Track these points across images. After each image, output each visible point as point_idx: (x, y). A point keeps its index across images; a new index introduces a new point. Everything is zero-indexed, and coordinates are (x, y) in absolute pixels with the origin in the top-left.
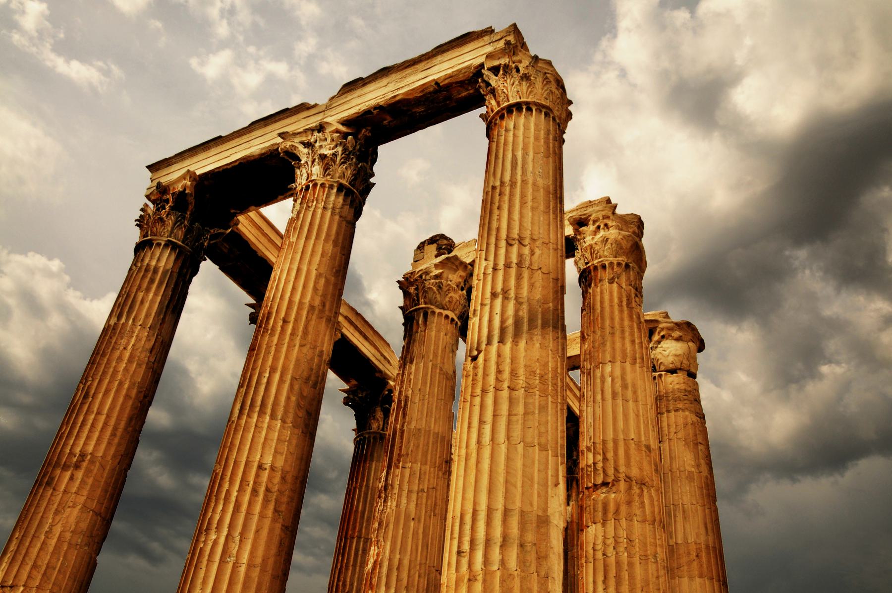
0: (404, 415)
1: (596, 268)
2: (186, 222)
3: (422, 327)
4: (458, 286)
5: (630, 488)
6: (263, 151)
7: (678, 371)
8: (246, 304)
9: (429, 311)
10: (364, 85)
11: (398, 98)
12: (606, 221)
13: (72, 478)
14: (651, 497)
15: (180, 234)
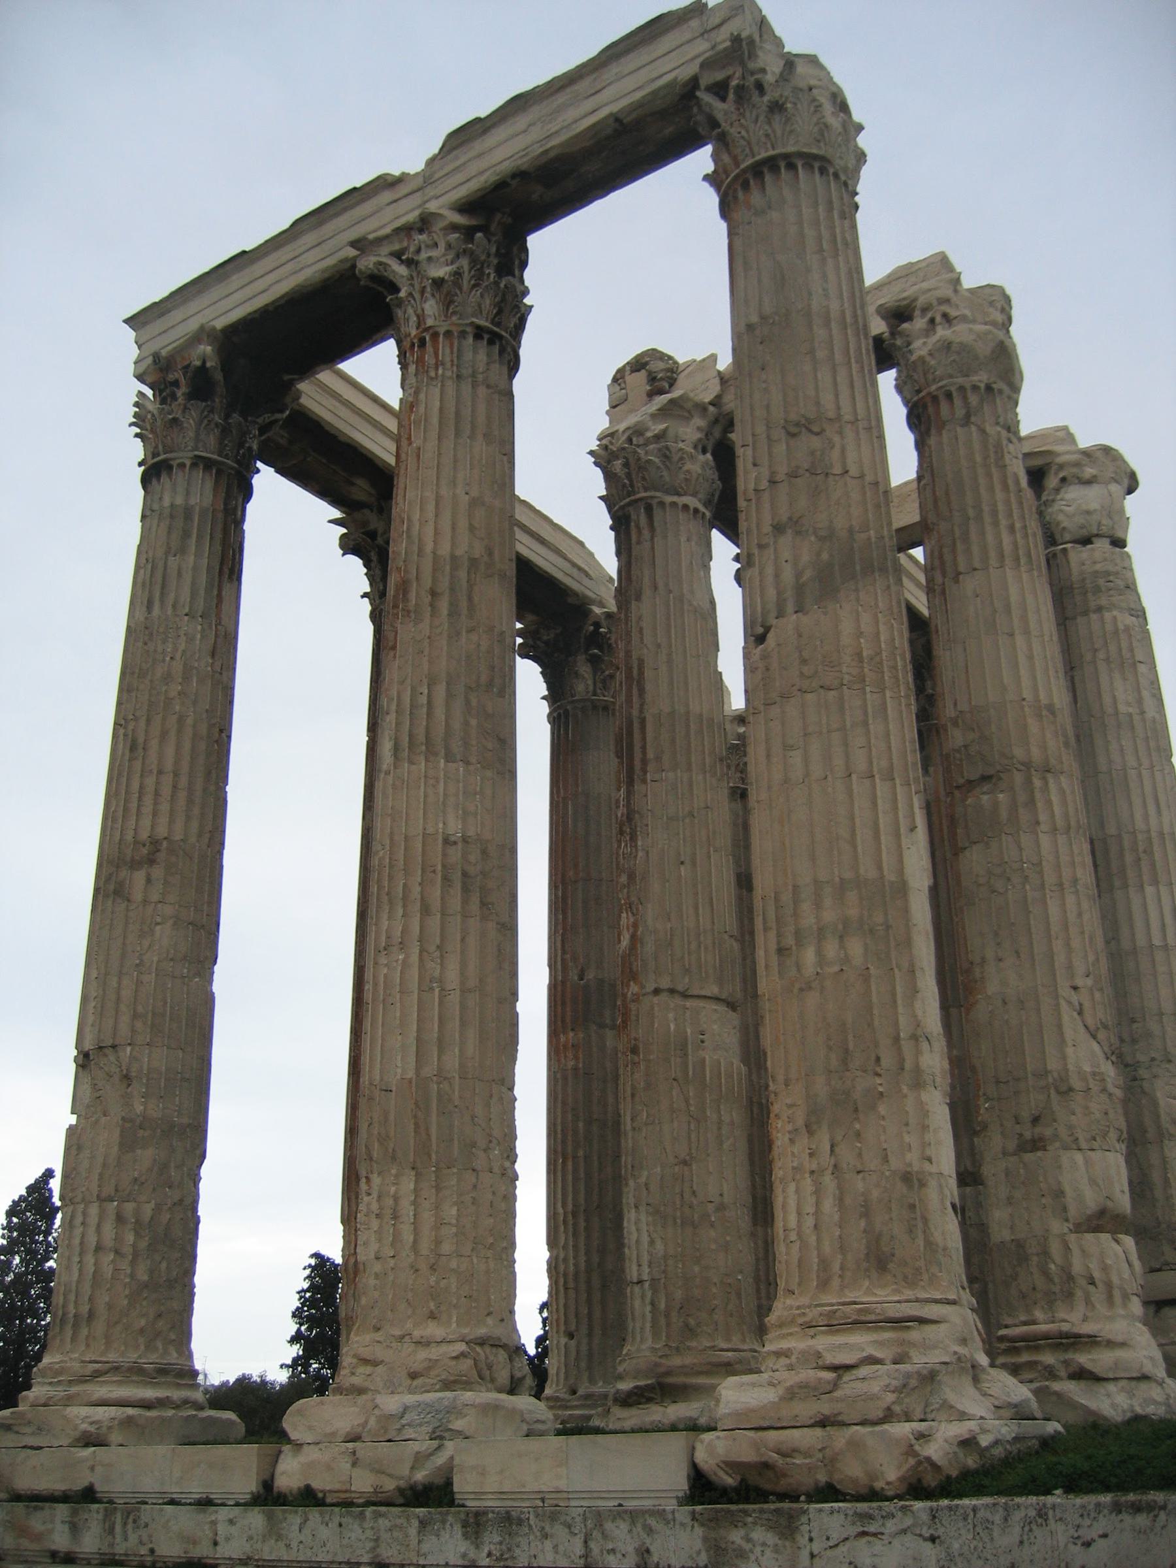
0: (642, 691)
1: (935, 399)
2: (217, 418)
3: (646, 533)
4: (695, 447)
5: (1029, 781)
6: (326, 275)
7: (1094, 539)
8: (330, 521)
9: (654, 502)
10: (485, 131)
11: (552, 154)
12: (945, 308)
13: (149, 880)
14: (1062, 791)
15: (212, 440)
